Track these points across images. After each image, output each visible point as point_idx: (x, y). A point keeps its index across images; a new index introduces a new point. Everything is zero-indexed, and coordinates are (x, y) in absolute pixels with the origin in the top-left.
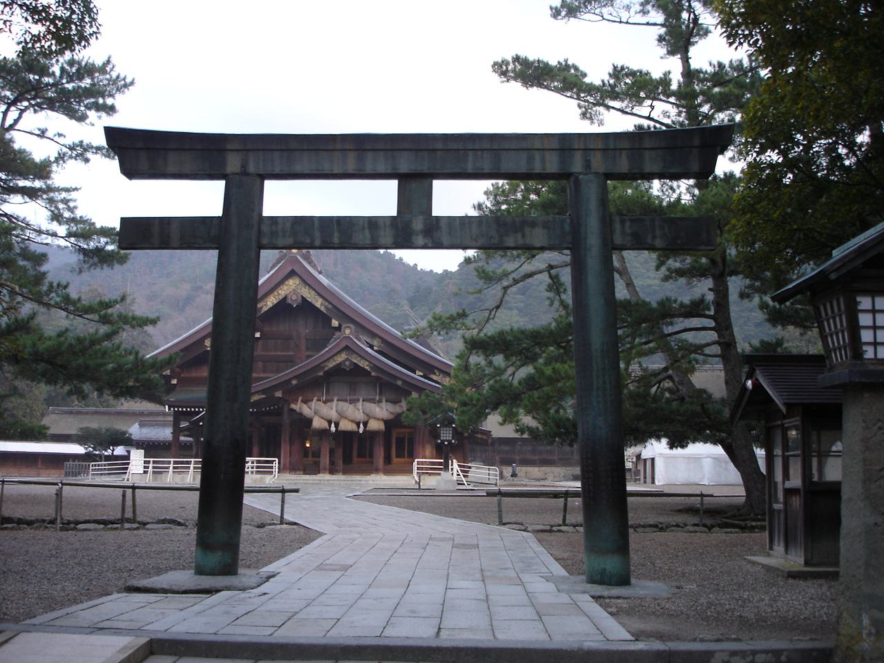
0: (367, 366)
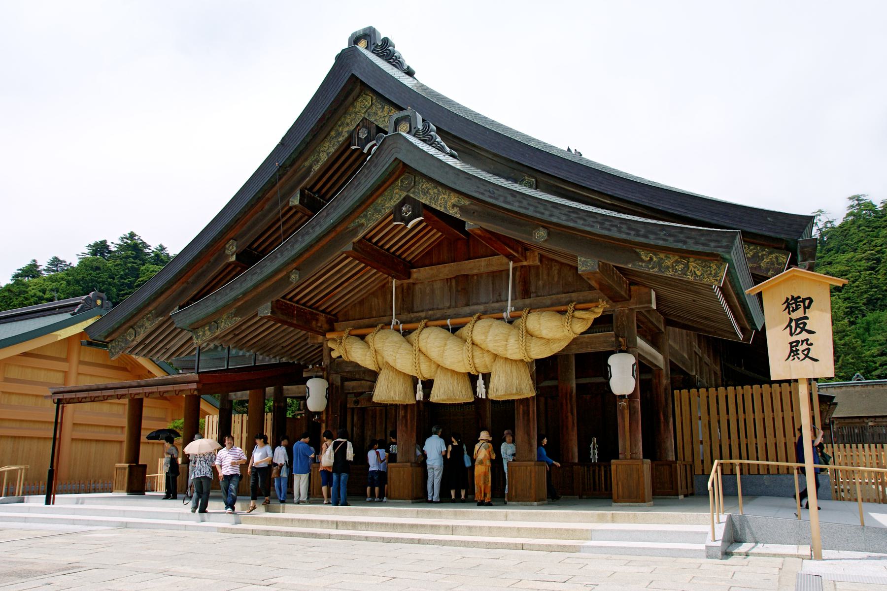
0: (454, 206)
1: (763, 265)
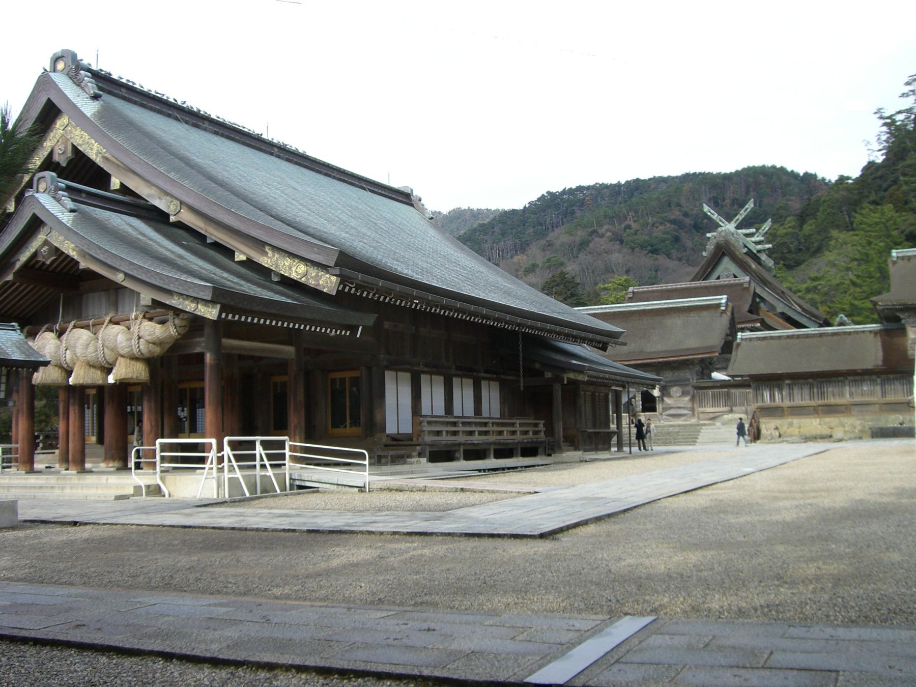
1: (321, 282)
